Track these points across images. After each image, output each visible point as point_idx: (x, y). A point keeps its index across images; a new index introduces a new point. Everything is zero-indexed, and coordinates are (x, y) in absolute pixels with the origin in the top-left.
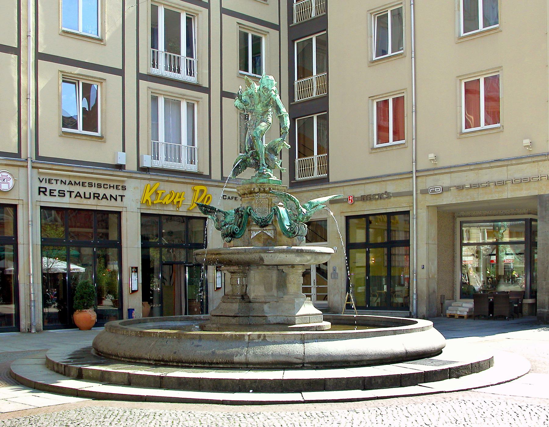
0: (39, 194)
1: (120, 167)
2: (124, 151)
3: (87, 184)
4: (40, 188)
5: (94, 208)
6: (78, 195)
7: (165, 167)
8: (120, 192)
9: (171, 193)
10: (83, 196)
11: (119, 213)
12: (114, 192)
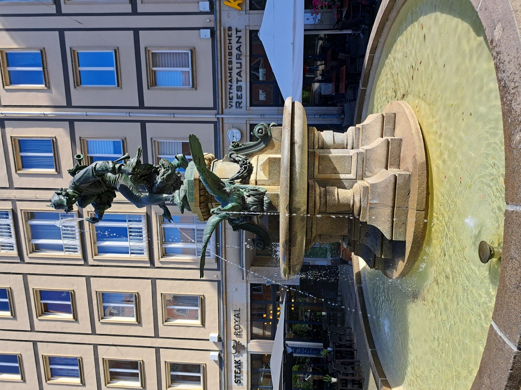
5: (248, 58)
6: (239, 74)
12: (234, 39)
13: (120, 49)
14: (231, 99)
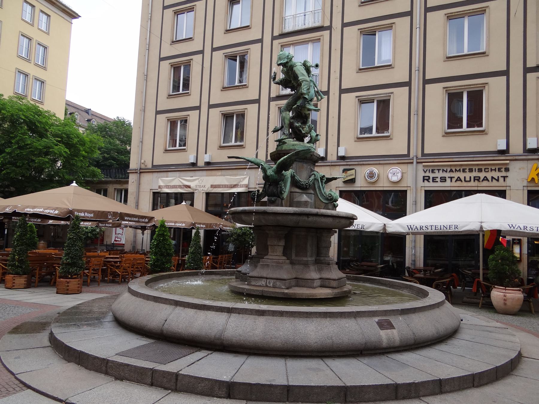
0: (424, 181)
3: (467, 170)
4: (424, 177)
6: (459, 179)
8: (504, 174)
10: (463, 180)
13: (486, 58)
14: (433, 171)
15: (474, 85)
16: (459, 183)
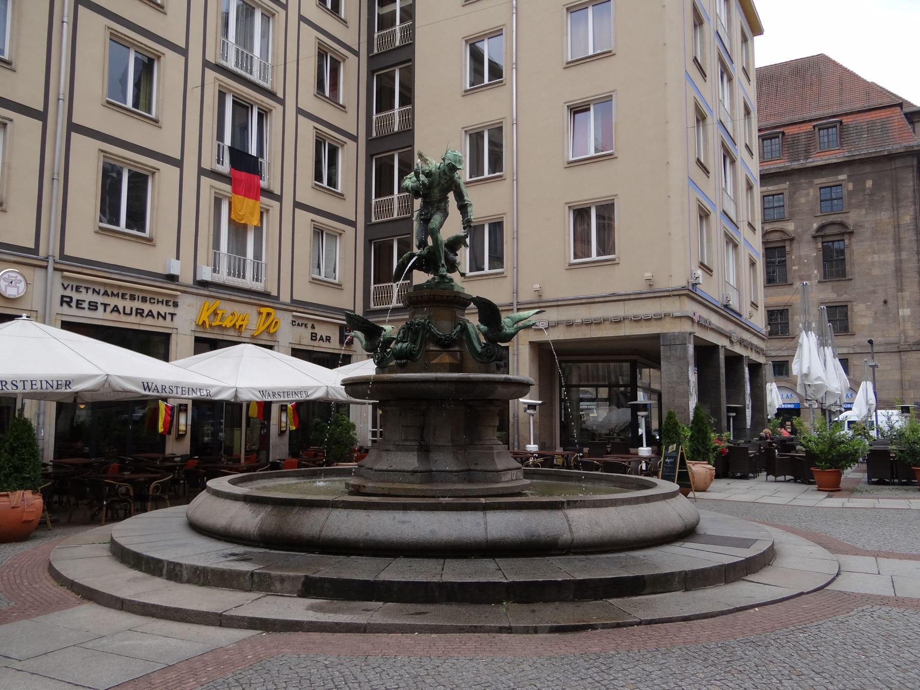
0: (62, 305)
1: (172, 278)
2: (178, 258)
3: (128, 297)
4: (63, 297)
5: (136, 327)
6: (116, 309)
7: (227, 283)
8: (171, 310)
9: (233, 314)
10: (121, 310)
11: (168, 336)
12: (163, 309)
14: (78, 289)
15: (142, 164)
16: (115, 316)
